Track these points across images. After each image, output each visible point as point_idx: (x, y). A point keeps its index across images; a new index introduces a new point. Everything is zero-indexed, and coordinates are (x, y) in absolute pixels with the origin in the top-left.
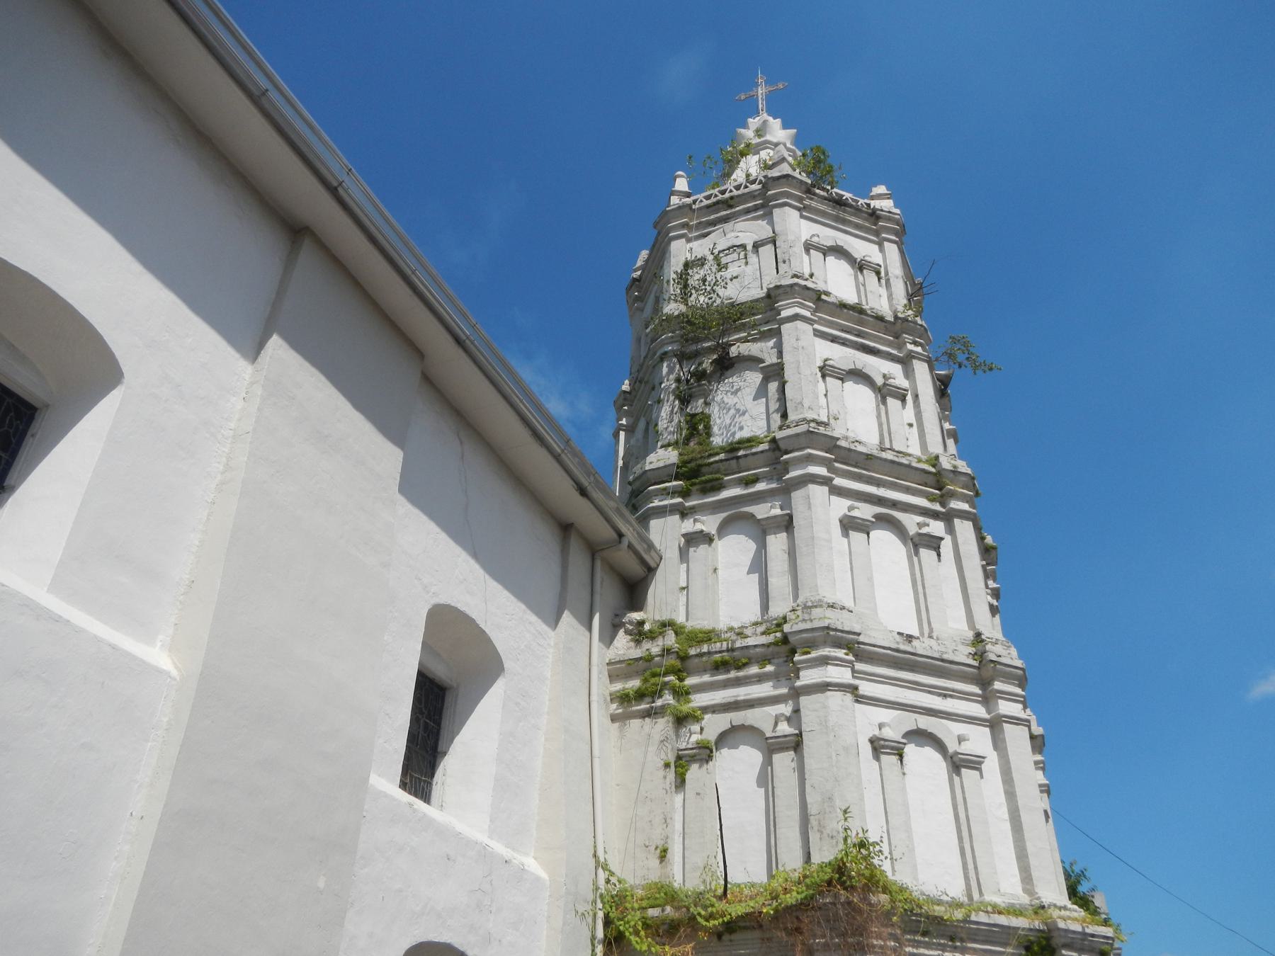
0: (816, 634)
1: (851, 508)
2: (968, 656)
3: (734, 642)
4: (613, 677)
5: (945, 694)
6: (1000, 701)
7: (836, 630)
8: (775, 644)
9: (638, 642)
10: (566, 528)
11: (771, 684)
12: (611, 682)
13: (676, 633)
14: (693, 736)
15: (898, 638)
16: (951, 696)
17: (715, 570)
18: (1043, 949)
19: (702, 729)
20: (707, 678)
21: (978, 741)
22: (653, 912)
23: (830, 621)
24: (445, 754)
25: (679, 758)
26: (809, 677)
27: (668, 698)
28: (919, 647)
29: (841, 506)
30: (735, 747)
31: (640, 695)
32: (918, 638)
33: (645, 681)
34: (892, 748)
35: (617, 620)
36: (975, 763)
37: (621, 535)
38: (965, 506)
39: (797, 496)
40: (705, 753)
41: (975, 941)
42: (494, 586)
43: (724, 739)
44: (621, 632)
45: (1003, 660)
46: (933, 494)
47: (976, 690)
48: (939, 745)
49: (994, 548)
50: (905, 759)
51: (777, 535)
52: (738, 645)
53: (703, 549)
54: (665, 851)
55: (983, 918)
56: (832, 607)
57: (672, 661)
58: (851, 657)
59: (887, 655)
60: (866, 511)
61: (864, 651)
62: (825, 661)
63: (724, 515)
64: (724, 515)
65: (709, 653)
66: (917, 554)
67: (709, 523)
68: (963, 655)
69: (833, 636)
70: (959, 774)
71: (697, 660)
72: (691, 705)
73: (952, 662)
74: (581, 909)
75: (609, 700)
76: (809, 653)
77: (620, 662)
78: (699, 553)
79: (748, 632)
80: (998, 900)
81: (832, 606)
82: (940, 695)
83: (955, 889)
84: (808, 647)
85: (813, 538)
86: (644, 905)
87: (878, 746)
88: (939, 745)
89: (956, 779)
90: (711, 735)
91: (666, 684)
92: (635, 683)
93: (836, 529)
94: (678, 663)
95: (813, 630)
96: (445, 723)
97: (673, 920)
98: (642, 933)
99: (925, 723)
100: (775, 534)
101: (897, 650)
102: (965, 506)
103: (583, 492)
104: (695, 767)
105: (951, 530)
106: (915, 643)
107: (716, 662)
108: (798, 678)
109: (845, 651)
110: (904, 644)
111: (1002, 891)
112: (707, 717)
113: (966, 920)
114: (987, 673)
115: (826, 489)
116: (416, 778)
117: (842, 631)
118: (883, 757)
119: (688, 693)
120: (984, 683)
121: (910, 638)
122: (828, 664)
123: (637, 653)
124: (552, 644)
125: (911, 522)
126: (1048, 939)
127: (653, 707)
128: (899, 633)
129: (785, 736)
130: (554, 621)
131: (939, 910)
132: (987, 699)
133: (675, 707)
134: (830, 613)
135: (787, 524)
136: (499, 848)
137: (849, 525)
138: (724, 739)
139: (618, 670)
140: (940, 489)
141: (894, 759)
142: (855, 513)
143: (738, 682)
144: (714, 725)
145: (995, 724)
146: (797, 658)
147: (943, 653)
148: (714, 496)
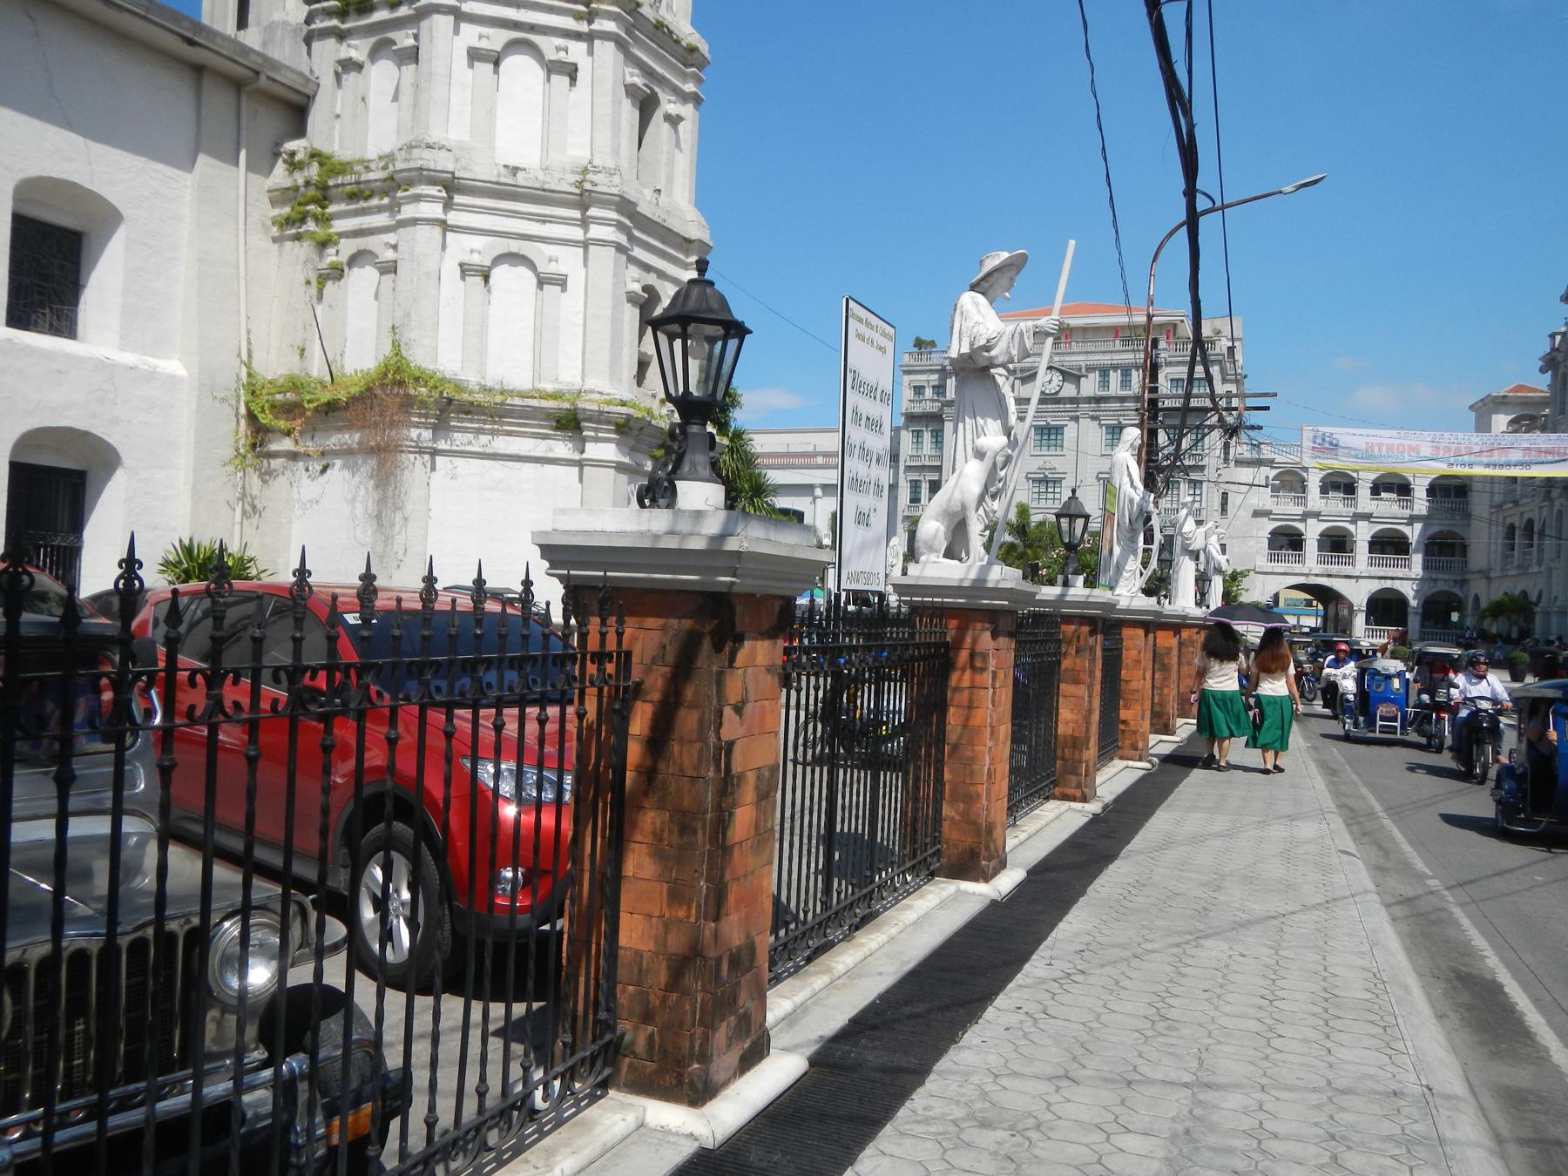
1: (481, 37)
2: (571, 185)
3: (360, 176)
4: (274, 203)
5: (544, 219)
6: (592, 226)
8: (385, 180)
9: (291, 173)
10: (198, 70)
11: (387, 214)
12: (273, 207)
13: (321, 164)
14: (331, 256)
15: (503, 170)
16: (550, 222)
17: (363, 99)
18: (571, 421)
19: (338, 252)
20: (342, 207)
21: (567, 261)
22: (279, 397)
24: (84, 286)
25: (320, 276)
26: (408, 211)
27: (311, 226)
28: (521, 179)
29: (471, 35)
30: (362, 267)
31: (288, 222)
32: (525, 170)
33: (293, 209)
34: (477, 271)
35: (275, 150)
36: (562, 282)
37: (257, 73)
38: (610, 26)
39: (424, 24)
40: (337, 273)
41: (512, 417)
42: (97, 148)
43: (354, 260)
44: (280, 161)
45: (599, 189)
46: (579, 12)
47: (577, 214)
48: (531, 265)
49: (693, 50)
50: (492, 280)
51: (410, 67)
52: (363, 179)
53: (353, 74)
54: (303, 350)
55: (517, 401)
56: (430, 147)
57: (312, 192)
58: (444, 194)
59: (488, 188)
60: (496, 39)
61: (464, 185)
62: (418, 198)
63: (373, 40)
64: (373, 40)
65: (343, 185)
66: (549, 80)
67: (357, 49)
68: (566, 184)
69: (426, 176)
70: (542, 289)
71: (334, 190)
72: (332, 230)
73: (553, 191)
74: (220, 395)
75: (269, 223)
76: (407, 190)
77: (276, 190)
78: (350, 79)
79: (373, 166)
80: (549, 387)
81: (429, 147)
82: (538, 221)
83: (520, 379)
84: (409, 185)
85: (430, 73)
86: (273, 391)
87: (465, 270)
88: (531, 265)
89: (540, 292)
90: (343, 258)
91: (308, 212)
92: (286, 210)
93: (461, 58)
94: (319, 194)
95: (409, 170)
96: (84, 262)
97: (294, 402)
98: (267, 412)
99: (515, 246)
100: (407, 64)
101: (498, 183)
102: (610, 26)
103: (191, 43)
104: (330, 283)
105: (591, 52)
106: (520, 175)
107: (347, 194)
108: (399, 211)
109: (439, 188)
110: (505, 177)
111: (560, 379)
112: (342, 241)
113: (502, 404)
114: (586, 200)
115: (451, 18)
116: (57, 309)
117: (436, 171)
118: (467, 278)
119: (327, 219)
120: (584, 207)
121: (515, 170)
123: (288, 183)
124: (189, 184)
125: (548, 45)
126: (575, 415)
127: (298, 233)
128: (505, 166)
130: (189, 164)
131: (479, 397)
132: (584, 223)
133: (313, 233)
134: (426, 154)
135: (412, 56)
136: (129, 358)
137: (475, 55)
138: (354, 260)
139: (280, 196)
140: (587, 6)
141: (479, 280)
142: (484, 44)
144: (348, 247)
145: (585, 245)
147: (545, 183)
148: (367, 18)
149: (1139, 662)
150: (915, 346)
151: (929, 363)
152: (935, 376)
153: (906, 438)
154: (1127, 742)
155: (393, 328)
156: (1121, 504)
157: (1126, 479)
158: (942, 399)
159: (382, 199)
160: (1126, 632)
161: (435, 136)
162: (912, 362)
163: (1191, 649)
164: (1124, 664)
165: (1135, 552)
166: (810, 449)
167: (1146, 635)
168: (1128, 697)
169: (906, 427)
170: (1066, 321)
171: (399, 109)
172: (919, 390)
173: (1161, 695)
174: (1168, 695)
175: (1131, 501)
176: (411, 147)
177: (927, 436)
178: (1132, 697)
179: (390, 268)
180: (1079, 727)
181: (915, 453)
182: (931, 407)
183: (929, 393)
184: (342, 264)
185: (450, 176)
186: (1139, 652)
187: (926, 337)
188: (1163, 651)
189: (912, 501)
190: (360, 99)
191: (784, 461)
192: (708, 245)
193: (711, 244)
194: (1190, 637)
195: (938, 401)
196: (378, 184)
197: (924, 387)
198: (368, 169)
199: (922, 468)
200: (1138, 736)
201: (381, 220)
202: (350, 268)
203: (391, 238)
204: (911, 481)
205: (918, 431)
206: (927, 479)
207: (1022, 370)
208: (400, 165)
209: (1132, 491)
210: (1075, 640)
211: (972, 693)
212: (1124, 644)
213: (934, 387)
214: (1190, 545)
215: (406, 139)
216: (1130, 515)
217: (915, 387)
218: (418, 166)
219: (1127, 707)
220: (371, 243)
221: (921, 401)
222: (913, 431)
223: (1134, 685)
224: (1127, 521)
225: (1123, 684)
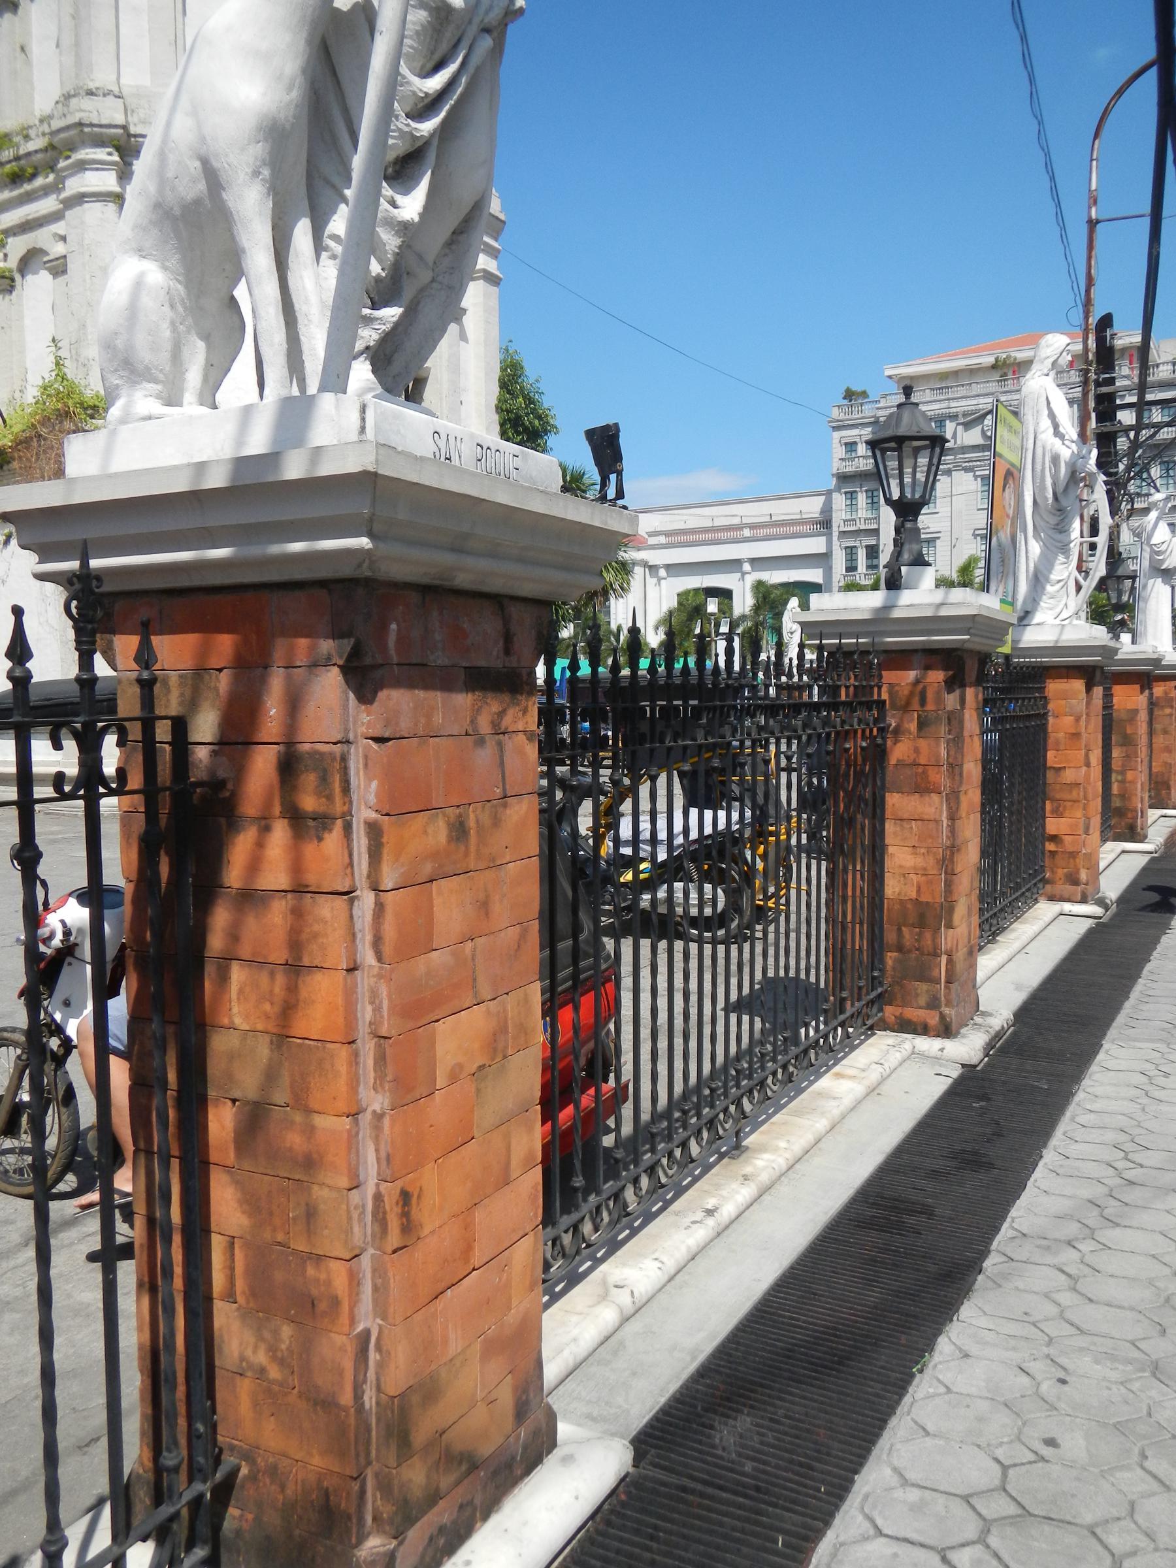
0: (73, 132)
3: (17, 146)
7: (92, 125)
17: (23, 49)
19: (6, 255)
23: (82, 115)
26: (74, 185)
30: (36, 273)
52: (21, 152)
69: (90, 134)
76: (68, 157)
79: (32, 133)
81: (90, 93)
84: (71, 150)
90: (13, 263)
112: (10, 240)
117: (101, 126)
122: (87, 169)
129: (57, 259)
143: (29, 198)
146: (62, 164)
149: (1076, 736)
150: (845, 398)
151: (860, 415)
153: (839, 500)
154: (1061, 872)
155: (54, 340)
156: (1039, 467)
157: (1046, 423)
159: (47, 177)
160: (1054, 687)
161: (102, 77)
162: (842, 416)
163: (1168, 711)
164: (1051, 741)
165: (1064, 549)
166: (736, 521)
167: (1089, 689)
168: (1058, 796)
169: (838, 489)
170: (1013, 354)
171: (60, 53)
172: (850, 446)
173: (1123, 782)
174: (1133, 782)
175: (1055, 459)
176: (67, 97)
177: (862, 498)
178: (1066, 796)
179: (59, 268)
180: (929, 882)
181: (849, 517)
184: (11, 271)
185: (120, 131)
186: (1078, 720)
187: (857, 388)
188: (1124, 716)
189: (849, 569)
190: (18, 49)
191: (709, 536)
192: (497, 218)
193: (502, 217)
194: (1166, 693)
196: (40, 156)
197: (855, 443)
198: (27, 138)
199: (858, 532)
200: (1080, 861)
201: (48, 204)
202: (23, 276)
203: (59, 228)
204: (846, 548)
205: (852, 493)
206: (865, 543)
207: (965, 415)
208: (57, 124)
209: (1057, 441)
210: (916, 701)
211: (297, 913)
212: (1050, 706)
214: (1163, 561)
215: (69, 87)
216: (1054, 484)
217: (846, 444)
218: (77, 120)
219: (1058, 813)
220: (42, 238)
221: (853, 459)
222: (846, 493)
223: (1069, 776)
224: (1050, 495)
225: (1050, 775)
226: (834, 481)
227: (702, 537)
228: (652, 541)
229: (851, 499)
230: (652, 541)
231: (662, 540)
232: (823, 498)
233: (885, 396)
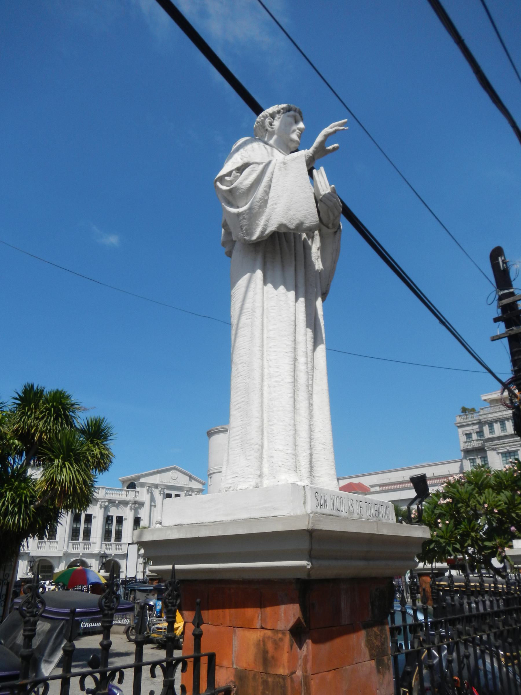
152: (476, 427)
158: (482, 438)
162: (462, 421)
169: (465, 458)
172: (468, 435)
182: (476, 444)
183: (474, 436)
187: (469, 406)
195: (481, 440)
205: (473, 459)
213: (477, 433)
222: (470, 459)
226: (462, 454)
227: (398, 486)
228: (372, 490)
229: (473, 462)
230: (372, 490)
231: (378, 489)
232: (460, 463)
233: (482, 409)
